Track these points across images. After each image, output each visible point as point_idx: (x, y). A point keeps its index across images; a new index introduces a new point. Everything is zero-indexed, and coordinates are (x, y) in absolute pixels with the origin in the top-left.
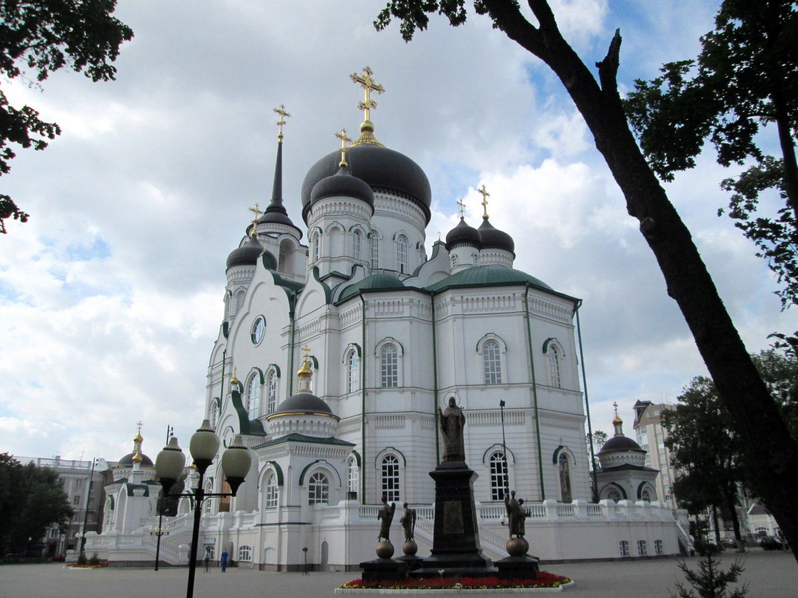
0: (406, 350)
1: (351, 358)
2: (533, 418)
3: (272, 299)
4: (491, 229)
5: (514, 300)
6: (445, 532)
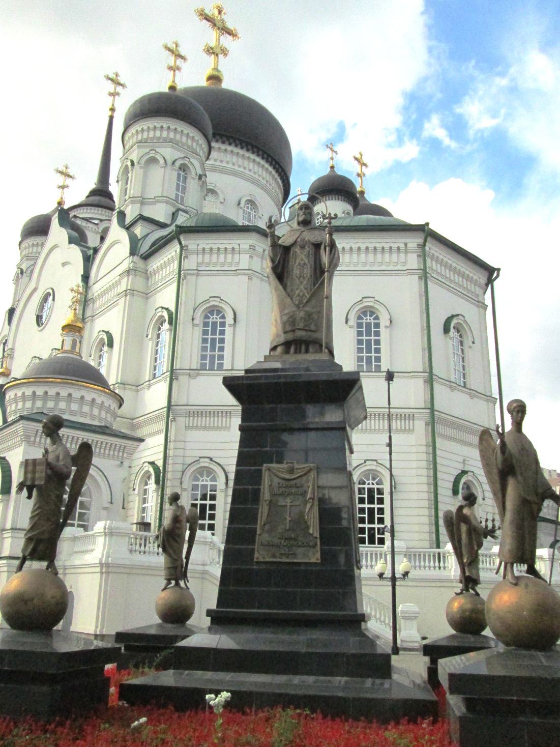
0: (241, 317)
1: (159, 329)
2: (427, 424)
3: (64, 264)
4: (366, 202)
6: (261, 555)
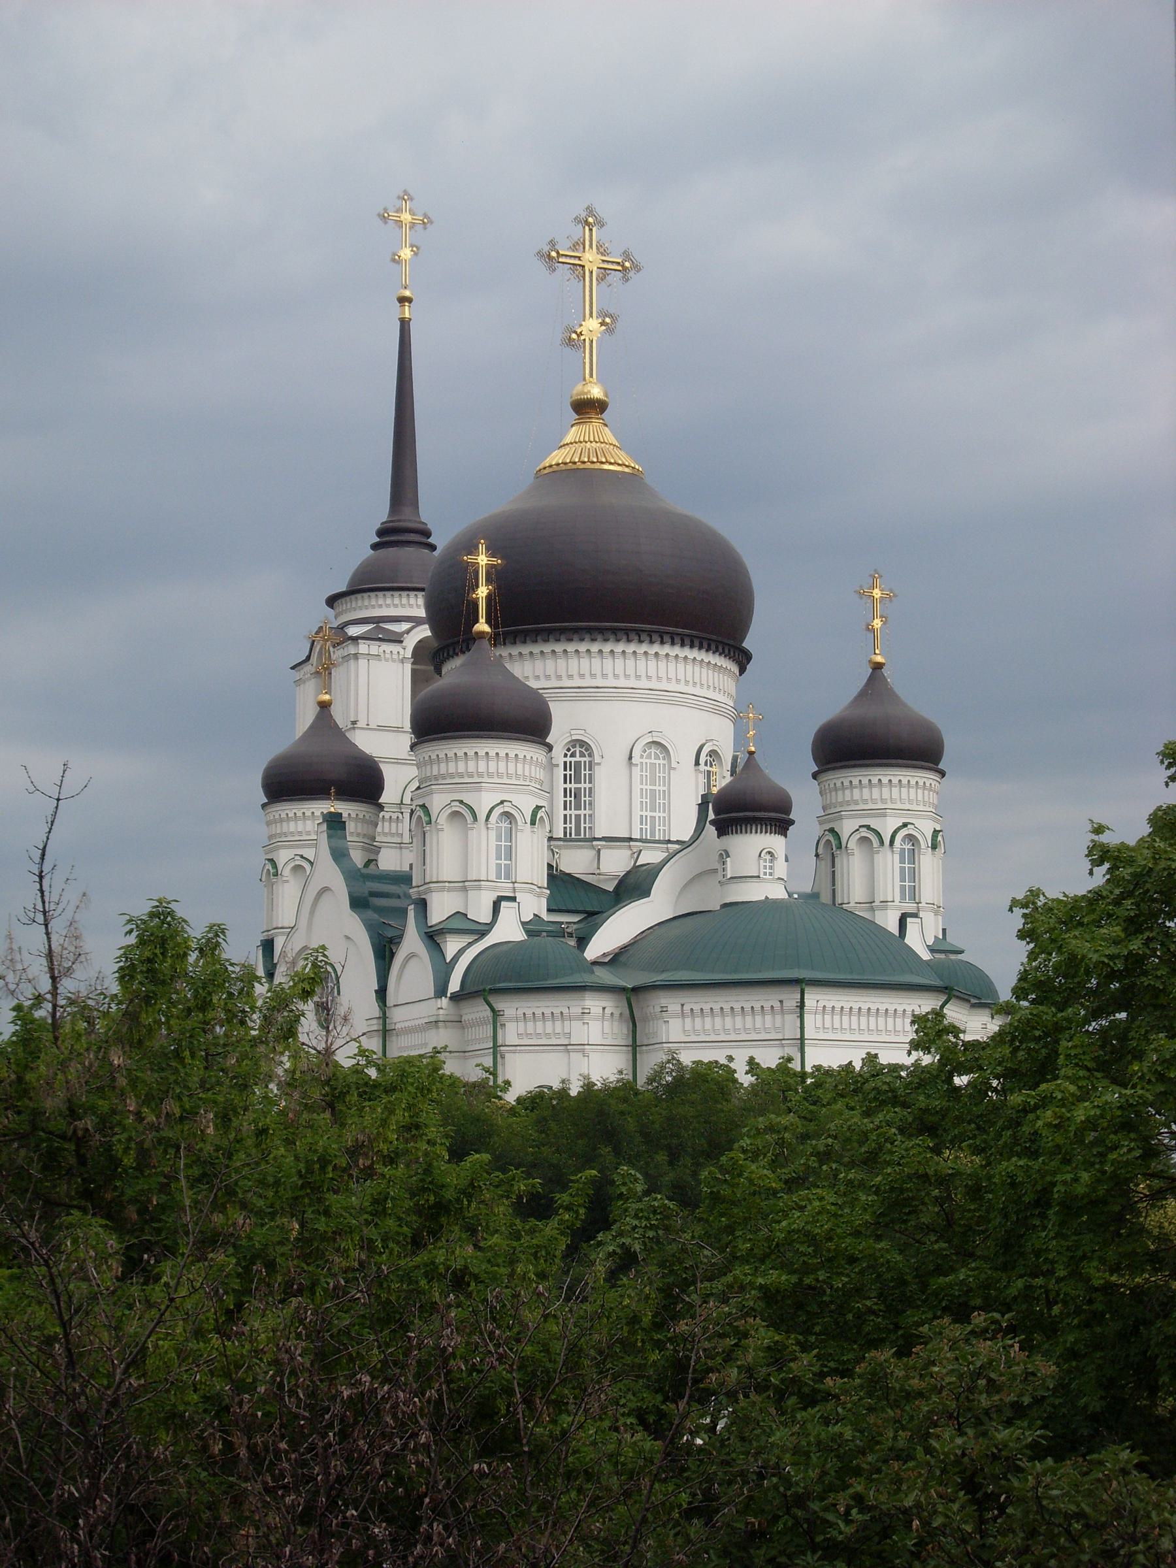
5: (782, 1011)
